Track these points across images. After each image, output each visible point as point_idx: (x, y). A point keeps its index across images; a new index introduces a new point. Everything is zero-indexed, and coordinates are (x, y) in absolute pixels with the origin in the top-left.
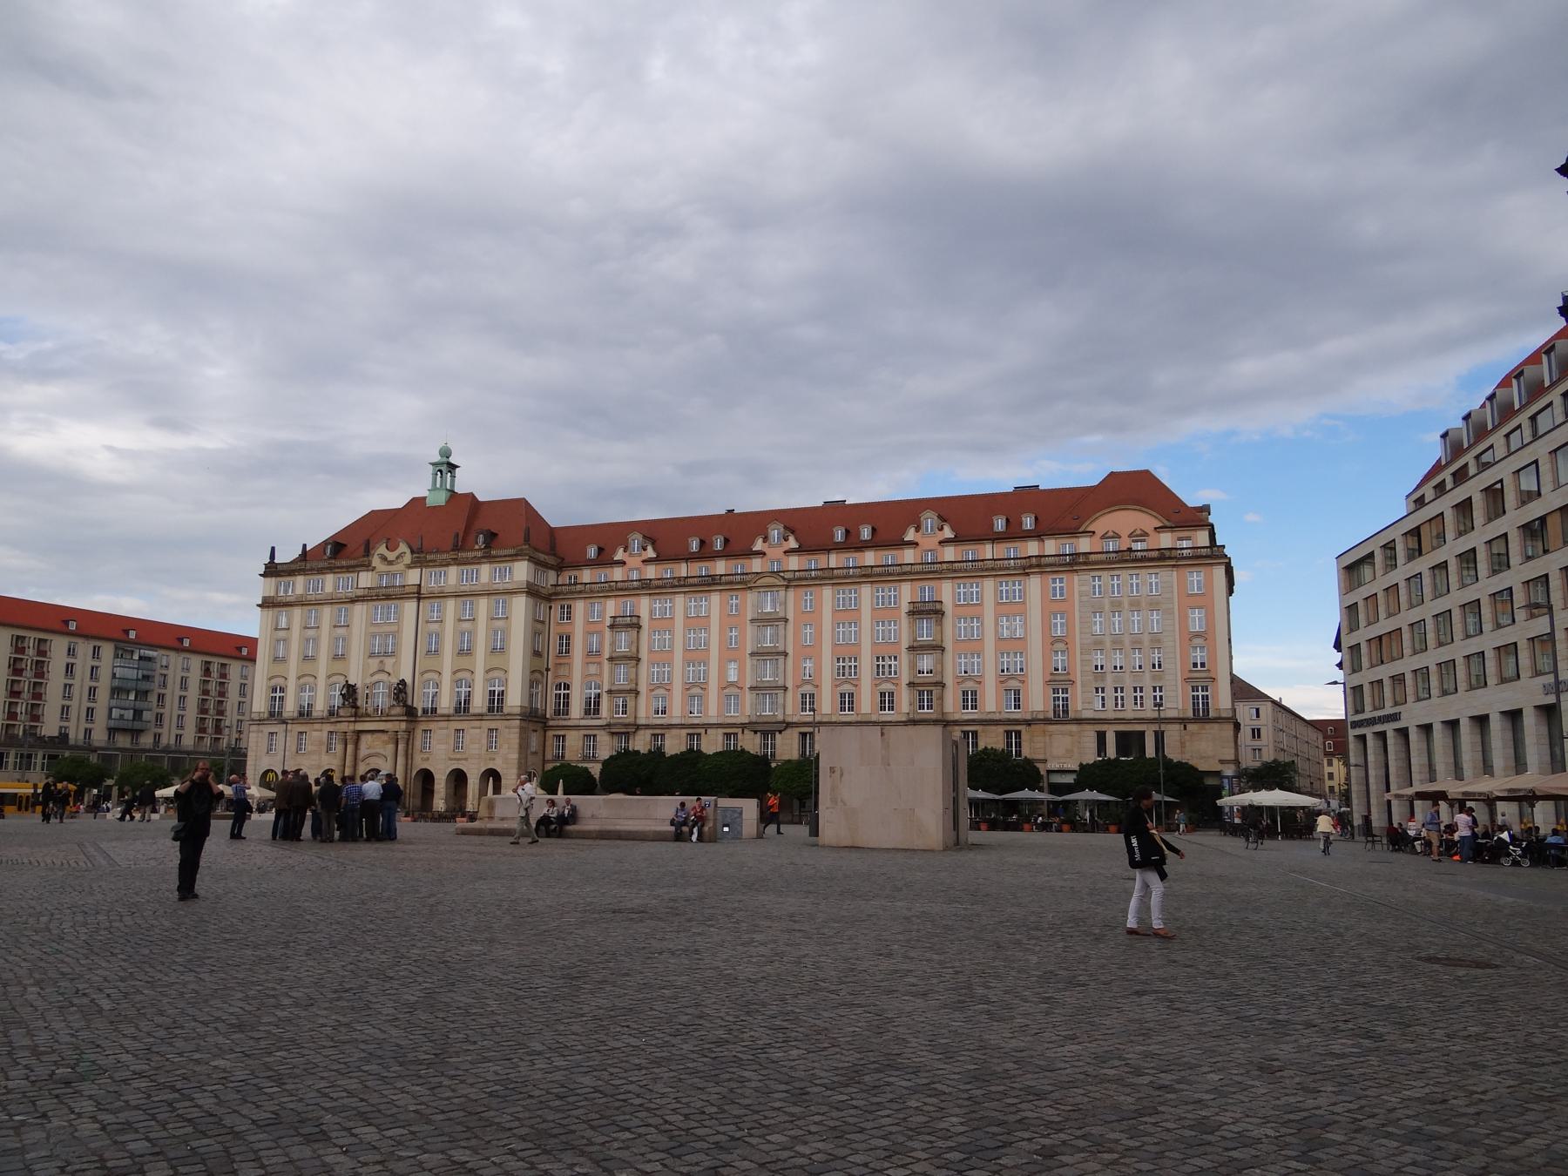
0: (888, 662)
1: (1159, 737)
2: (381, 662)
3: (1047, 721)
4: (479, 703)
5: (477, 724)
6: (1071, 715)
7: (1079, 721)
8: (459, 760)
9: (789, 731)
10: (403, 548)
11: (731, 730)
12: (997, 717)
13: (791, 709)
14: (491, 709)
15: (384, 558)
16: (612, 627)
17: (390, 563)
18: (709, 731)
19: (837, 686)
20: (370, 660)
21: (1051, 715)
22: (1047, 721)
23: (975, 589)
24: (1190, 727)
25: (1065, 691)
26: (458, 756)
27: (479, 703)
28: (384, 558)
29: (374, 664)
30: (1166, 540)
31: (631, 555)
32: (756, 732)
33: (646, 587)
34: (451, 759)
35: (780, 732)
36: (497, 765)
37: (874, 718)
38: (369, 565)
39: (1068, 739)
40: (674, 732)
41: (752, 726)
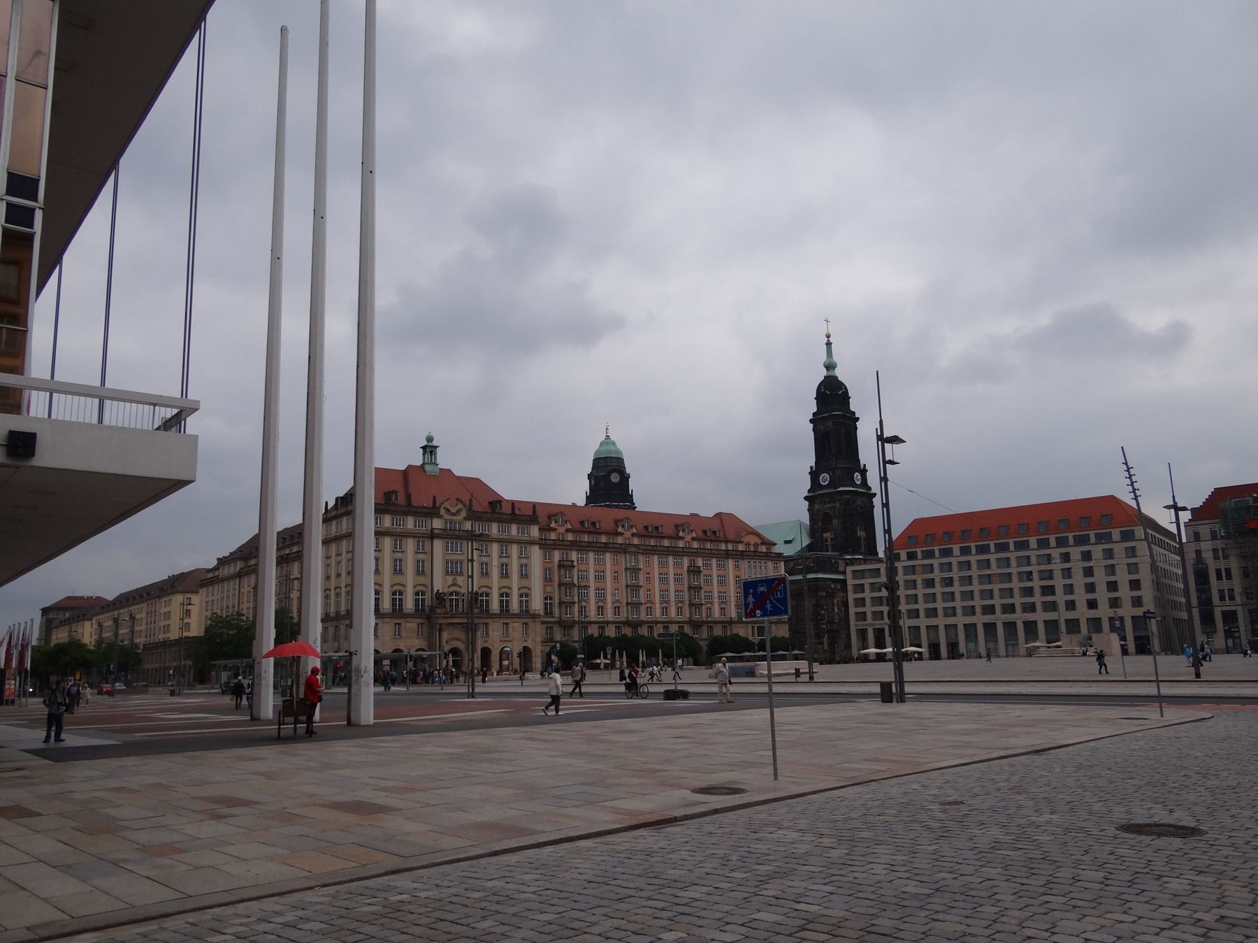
2: (454, 579)
4: (515, 606)
8: (506, 641)
9: (644, 625)
10: (460, 506)
11: (619, 625)
12: (719, 619)
13: (643, 616)
14: (502, 611)
15: (448, 510)
16: (560, 566)
17: (453, 514)
20: (447, 577)
24: (778, 625)
28: (448, 510)
29: (450, 579)
30: (763, 549)
32: (629, 626)
33: (574, 545)
34: (501, 641)
35: (640, 626)
36: (529, 644)
37: (676, 619)
38: (439, 513)
39: (743, 629)
40: (593, 625)
41: (627, 623)
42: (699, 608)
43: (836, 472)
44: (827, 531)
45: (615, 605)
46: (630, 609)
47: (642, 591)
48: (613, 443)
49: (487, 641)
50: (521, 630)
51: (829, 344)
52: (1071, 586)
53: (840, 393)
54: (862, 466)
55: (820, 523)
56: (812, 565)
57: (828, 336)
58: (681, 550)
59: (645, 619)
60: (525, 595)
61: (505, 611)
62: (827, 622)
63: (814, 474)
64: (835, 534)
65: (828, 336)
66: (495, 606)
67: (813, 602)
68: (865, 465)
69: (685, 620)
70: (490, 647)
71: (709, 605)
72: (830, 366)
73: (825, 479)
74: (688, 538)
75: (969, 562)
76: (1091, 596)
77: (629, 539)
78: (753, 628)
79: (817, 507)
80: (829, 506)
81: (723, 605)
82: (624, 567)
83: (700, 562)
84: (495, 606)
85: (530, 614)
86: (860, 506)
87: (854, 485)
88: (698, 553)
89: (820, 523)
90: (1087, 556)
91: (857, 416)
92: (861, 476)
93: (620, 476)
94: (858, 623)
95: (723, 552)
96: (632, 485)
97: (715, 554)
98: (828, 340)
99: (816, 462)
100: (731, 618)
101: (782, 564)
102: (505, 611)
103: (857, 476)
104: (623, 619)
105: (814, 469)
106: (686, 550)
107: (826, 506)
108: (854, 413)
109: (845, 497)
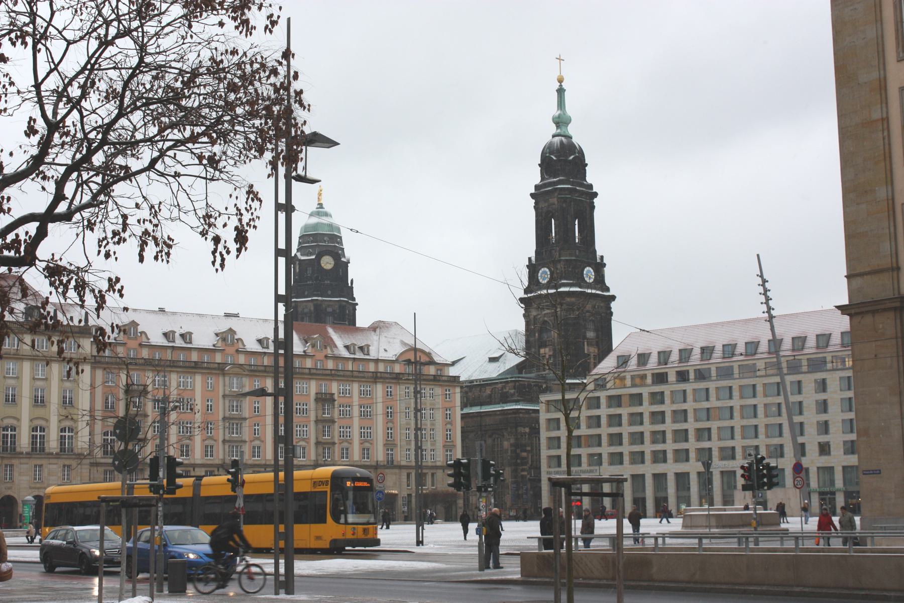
0: (302, 429)
1: (433, 475)
3: (385, 467)
4: (53, 444)
5: (55, 461)
6: (395, 463)
7: (400, 467)
8: (38, 488)
18: (196, 469)
19: (361, 444)
21: (386, 463)
22: (385, 467)
23: (305, 386)
25: (392, 450)
26: (38, 485)
27: (53, 444)
30: (432, 370)
31: (129, 338)
34: (30, 488)
42: (329, 449)
43: (559, 267)
44: (545, 346)
45: (207, 442)
46: (227, 450)
47: (246, 424)
48: (326, 214)
49: (10, 488)
50: (60, 474)
51: (561, 91)
52: (826, 423)
53: (571, 158)
54: (598, 260)
55: (537, 335)
56: (512, 391)
57: (560, 81)
58: (307, 371)
59: (250, 462)
60: (67, 431)
61: (38, 448)
62: (530, 468)
63: (533, 269)
64: (554, 350)
65: (560, 81)
66: (24, 442)
67: (512, 441)
68: (602, 257)
69: (308, 463)
70: (15, 496)
71: (345, 445)
72: (561, 121)
73: (544, 274)
74: (320, 356)
75: (641, 395)
76: (823, 439)
77: (232, 355)
78: (408, 475)
79: (534, 313)
80: (548, 311)
81: (367, 445)
82: (221, 394)
83: (334, 388)
84: (24, 442)
85: (75, 454)
86: (588, 311)
87: (580, 281)
88: (331, 375)
89: (537, 335)
90: (822, 386)
91: (594, 190)
92: (595, 272)
93: (335, 259)
94: (551, 470)
95: (370, 375)
96: (353, 273)
97: (358, 377)
98: (561, 86)
99: (537, 252)
100: (377, 461)
101: (458, 390)
102: (38, 448)
103: (589, 274)
104: (217, 462)
105: (533, 259)
106: (314, 371)
107: (544, 313)
108: (591, 187)
109: (568, 299)
